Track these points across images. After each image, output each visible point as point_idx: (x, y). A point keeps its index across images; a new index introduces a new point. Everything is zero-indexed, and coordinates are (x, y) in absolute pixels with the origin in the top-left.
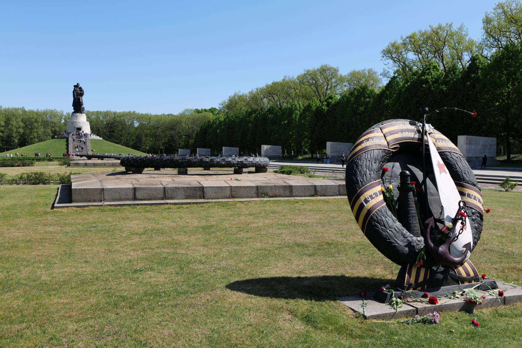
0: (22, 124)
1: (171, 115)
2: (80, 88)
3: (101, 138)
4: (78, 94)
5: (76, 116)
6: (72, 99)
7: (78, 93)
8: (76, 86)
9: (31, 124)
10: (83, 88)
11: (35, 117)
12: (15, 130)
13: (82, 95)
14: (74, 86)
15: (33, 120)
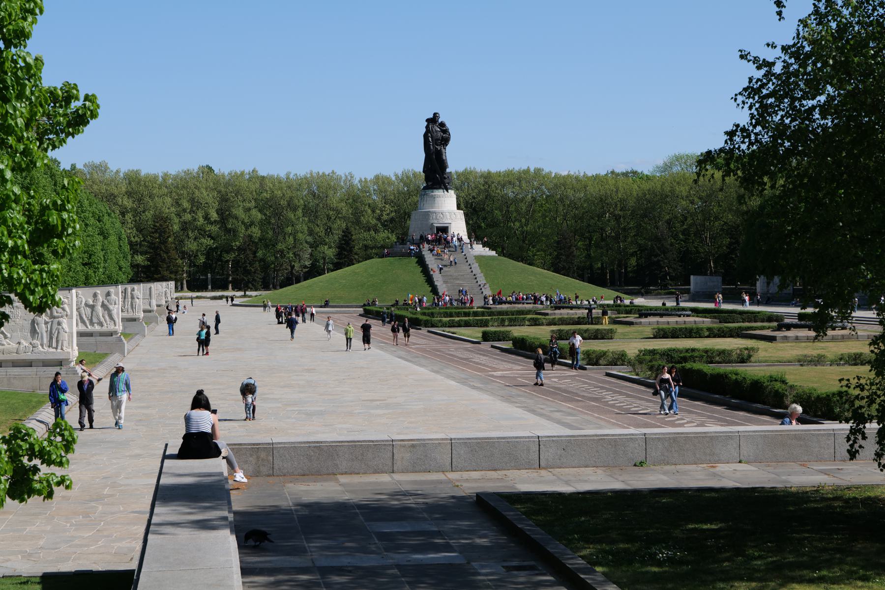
0: (257, 215)
1: (635, 173)
2: (442, 125)
3: (493, 253)
4: (436, 141)
5: (434, 197)
6: (424, 155)
7: (436, 137)
8: (433, 120)
9: (278, 214)
10: (449, 125)
11: (289, 194)
12: (242, 229)
13: (445, 141)
14: (428, 120)
15: (283, 203)
